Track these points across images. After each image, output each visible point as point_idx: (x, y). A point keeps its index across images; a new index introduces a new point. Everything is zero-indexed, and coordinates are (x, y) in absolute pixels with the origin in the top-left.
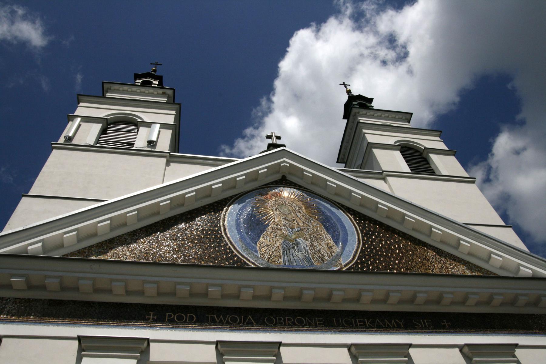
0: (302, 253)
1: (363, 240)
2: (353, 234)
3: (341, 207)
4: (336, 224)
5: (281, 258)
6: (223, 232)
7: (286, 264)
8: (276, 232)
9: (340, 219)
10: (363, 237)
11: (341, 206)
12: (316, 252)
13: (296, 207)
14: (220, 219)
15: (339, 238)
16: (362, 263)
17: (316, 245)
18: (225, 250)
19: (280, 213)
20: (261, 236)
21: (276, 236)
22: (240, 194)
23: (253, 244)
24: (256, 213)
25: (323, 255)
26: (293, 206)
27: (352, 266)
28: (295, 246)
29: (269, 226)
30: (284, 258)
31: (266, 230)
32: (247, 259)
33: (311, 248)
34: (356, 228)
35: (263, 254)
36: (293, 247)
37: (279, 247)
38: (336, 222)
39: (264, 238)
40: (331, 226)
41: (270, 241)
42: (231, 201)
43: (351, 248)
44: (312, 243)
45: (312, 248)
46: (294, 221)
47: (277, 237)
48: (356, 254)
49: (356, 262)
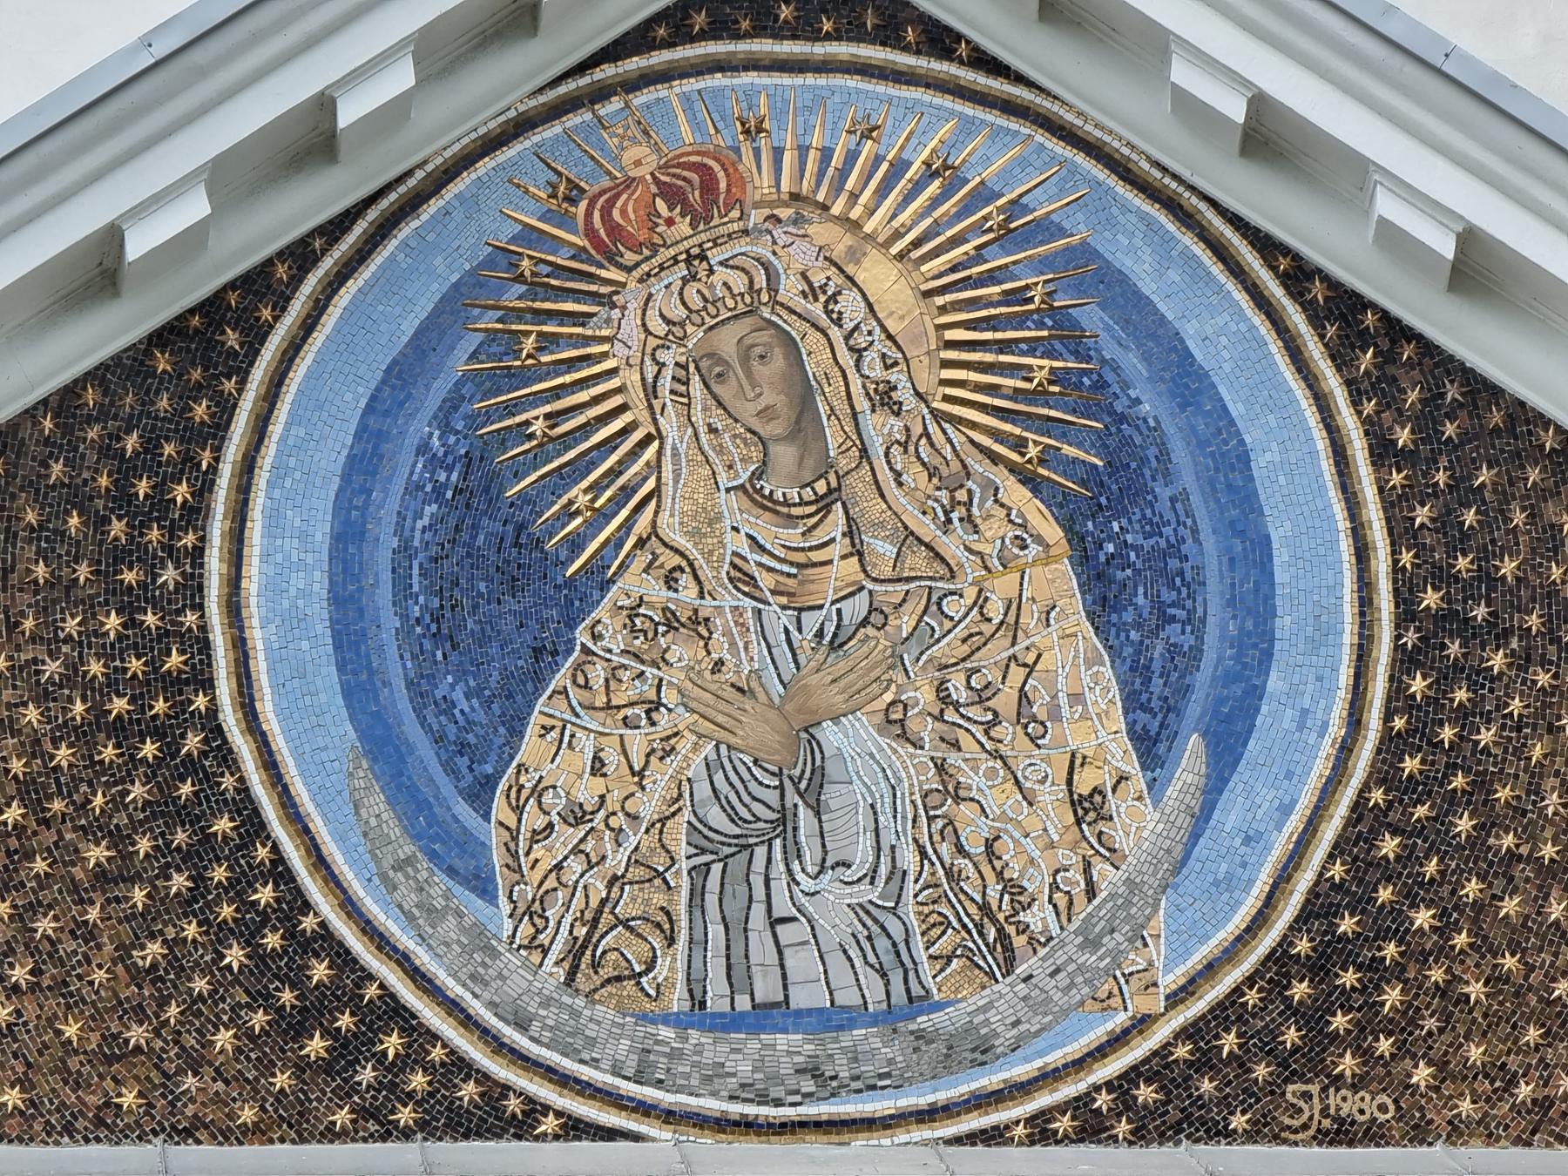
0: (849, 875)
1: (1398, 696)
2: (1324, 634)
3: (1275, 289)
4: (1195, 531)
5: (671, 941)
6: (225, 689)
7: (703, 1004)
8: (662, 661)
9: (1244, 459)
10: (1406, 661)
11: (1285, 279)
12: (961, 862)
13: (861, 340)
14: (198, 552)
15: (1188, 689)
16: (1319, 968)
17: (973, 780)
18: (238, 888)
19: (712, 430)
20: (535, 719)
21: (658, 705)
22: (384, 203)
23: (464, 811)
24: (504, 438)
25: (1013, 888)
26: (838, 322)
27: (1237, 991)
28: (801, 809)
29: (606, 585)
30: (698, 943)
31: (582, 636)
32: (404, 962)
33: (930, 819)
34: (1362, 553)
35: (533, 912)
36: (784, 821)
37: (669, 824)
38: (1196, 500)
39: (558, 730)
40: (1148, 545)
41: (598, 766)
42: (297, 307)
43: (1267, 798)
44: (941, 768)
45: (940, 823)
46: (827, 509)
47: (662, 717)
48: (1297, 868)
49: (1280, 957)
